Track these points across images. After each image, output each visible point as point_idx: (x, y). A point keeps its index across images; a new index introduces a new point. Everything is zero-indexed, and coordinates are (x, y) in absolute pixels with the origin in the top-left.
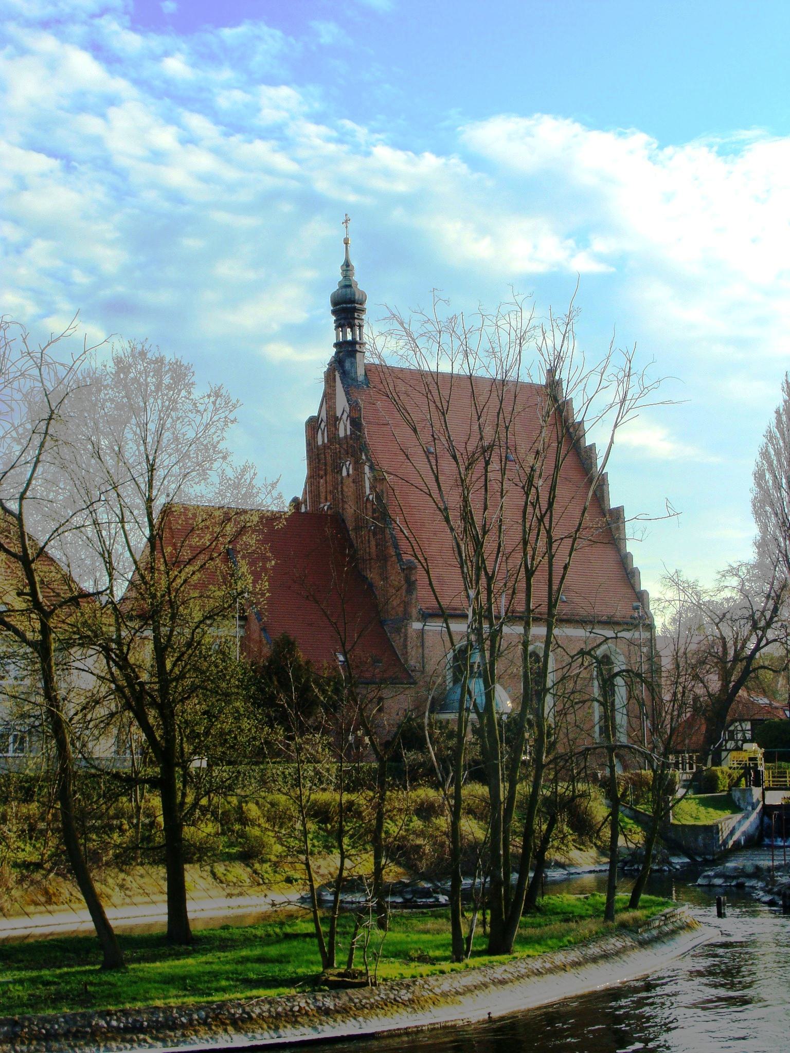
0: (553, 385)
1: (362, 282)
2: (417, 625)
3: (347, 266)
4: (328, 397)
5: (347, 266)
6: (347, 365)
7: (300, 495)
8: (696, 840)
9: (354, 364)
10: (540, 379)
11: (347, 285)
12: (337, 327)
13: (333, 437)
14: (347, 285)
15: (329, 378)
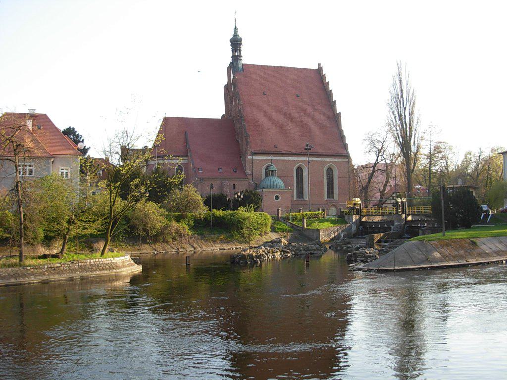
0: (320, 69)
1: (241, 34)
2: (250, 157)
3: (236, 29)
4: (229, 76)
5: (236, 29)
6: (235, 64)
7: (224, 113)
8: (313, 235)
9: (237, 64)
10: (316, 67)
11: (235, 35)
12: (232, 51)
13: (230, 91)
14: (235, 35)
15: (228, 68)
